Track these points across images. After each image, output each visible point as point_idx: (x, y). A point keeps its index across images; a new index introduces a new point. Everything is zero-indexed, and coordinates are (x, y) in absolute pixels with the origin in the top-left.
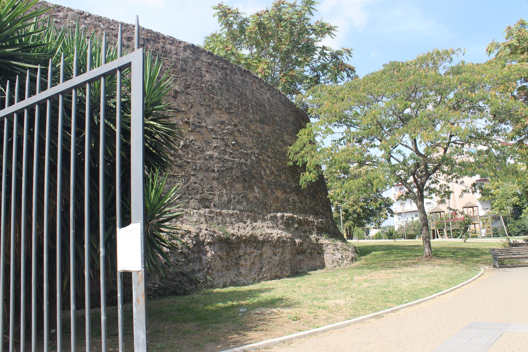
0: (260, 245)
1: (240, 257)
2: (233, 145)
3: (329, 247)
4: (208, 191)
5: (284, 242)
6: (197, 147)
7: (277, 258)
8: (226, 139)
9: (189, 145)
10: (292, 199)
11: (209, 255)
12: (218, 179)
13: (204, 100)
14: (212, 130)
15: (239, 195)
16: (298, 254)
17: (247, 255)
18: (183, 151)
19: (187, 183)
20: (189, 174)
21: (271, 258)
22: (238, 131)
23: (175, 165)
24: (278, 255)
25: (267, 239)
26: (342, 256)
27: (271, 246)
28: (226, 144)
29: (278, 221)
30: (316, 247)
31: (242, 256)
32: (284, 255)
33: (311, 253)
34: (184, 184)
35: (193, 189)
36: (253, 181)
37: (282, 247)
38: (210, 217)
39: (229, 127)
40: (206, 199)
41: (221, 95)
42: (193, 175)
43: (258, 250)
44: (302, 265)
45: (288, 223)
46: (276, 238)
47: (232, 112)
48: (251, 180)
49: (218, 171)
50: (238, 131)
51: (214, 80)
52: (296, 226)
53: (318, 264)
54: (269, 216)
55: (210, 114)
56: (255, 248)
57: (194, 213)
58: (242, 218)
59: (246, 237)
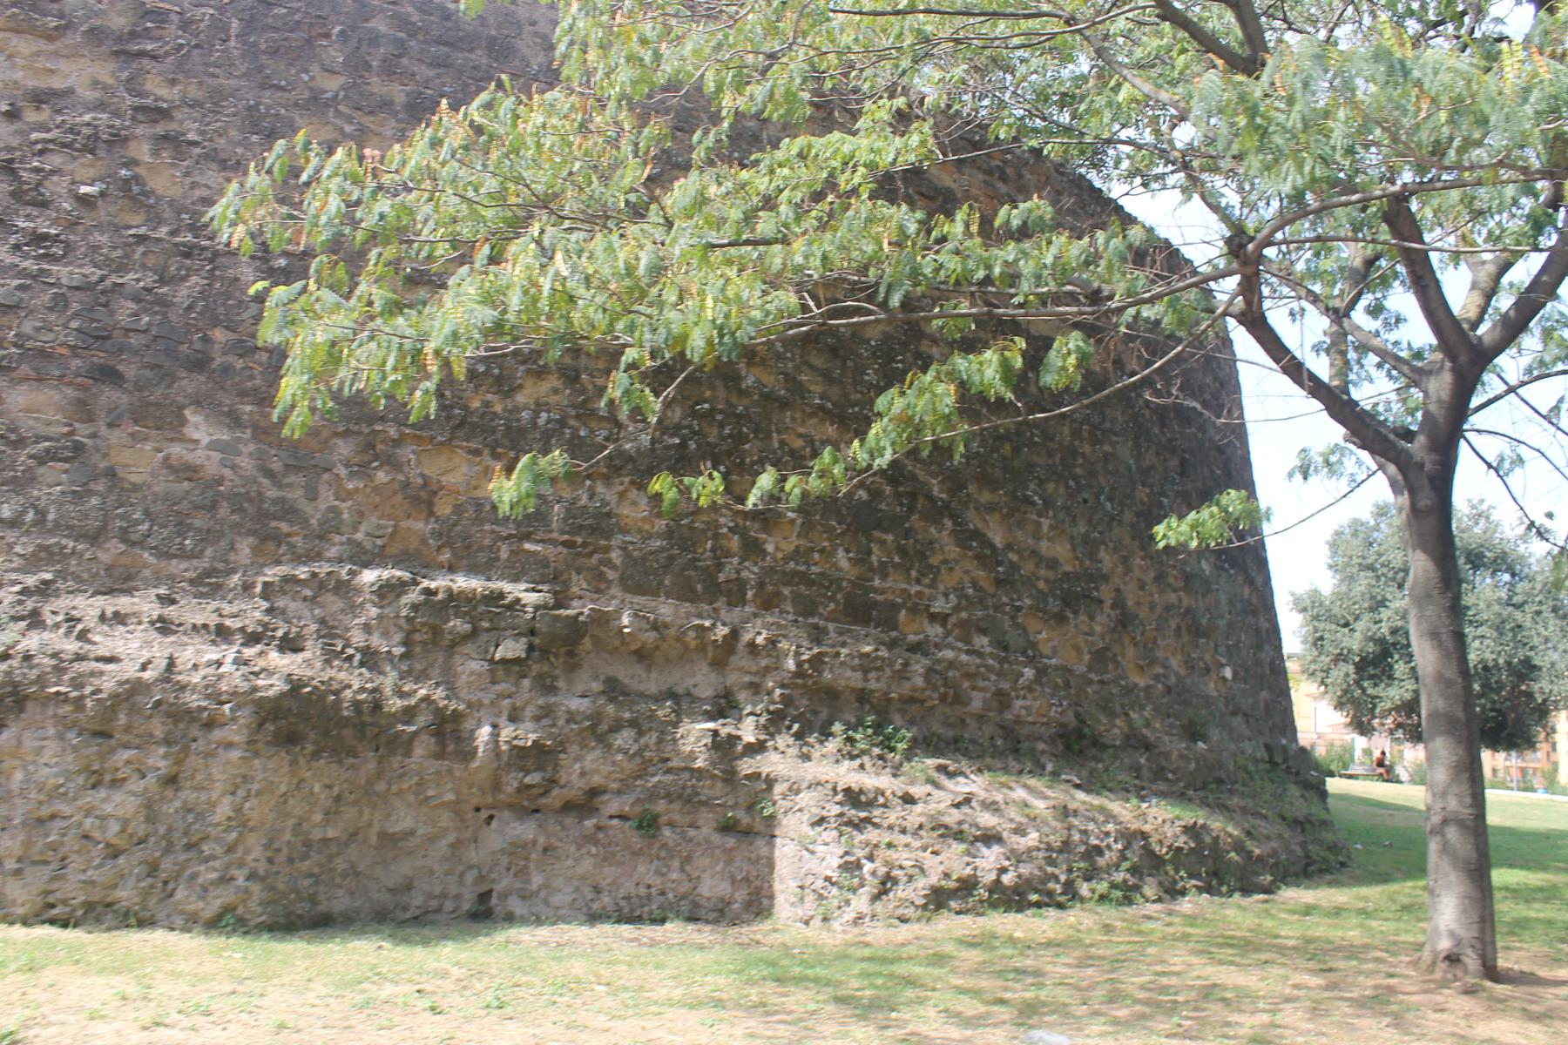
2: (85, 201)
3: (805, 798)
5: (179, 715)
7: (121, 804)
8: (37, 170)
10: (572, 511)
15: (20, 443)
16: (528, 806)
21: (54, 793)
22: (173, 143)
24: (136, 785)
25: (41, 681)
26: (852, 867)
27: (64, 724)
28: (16, 195)
29: (353, 609)
30: (713, 790)
32: (188, 795)
33: (648, 824)
36: (190, 383)
37: (167, 742)
44: (537, 880)
45: (436, 631)
46: (108, 685)
47: (142, 54)
48: (169, 377)
50: (173, 143)
52: (511, 648)
53: (712, 887)
54: (272, 574)
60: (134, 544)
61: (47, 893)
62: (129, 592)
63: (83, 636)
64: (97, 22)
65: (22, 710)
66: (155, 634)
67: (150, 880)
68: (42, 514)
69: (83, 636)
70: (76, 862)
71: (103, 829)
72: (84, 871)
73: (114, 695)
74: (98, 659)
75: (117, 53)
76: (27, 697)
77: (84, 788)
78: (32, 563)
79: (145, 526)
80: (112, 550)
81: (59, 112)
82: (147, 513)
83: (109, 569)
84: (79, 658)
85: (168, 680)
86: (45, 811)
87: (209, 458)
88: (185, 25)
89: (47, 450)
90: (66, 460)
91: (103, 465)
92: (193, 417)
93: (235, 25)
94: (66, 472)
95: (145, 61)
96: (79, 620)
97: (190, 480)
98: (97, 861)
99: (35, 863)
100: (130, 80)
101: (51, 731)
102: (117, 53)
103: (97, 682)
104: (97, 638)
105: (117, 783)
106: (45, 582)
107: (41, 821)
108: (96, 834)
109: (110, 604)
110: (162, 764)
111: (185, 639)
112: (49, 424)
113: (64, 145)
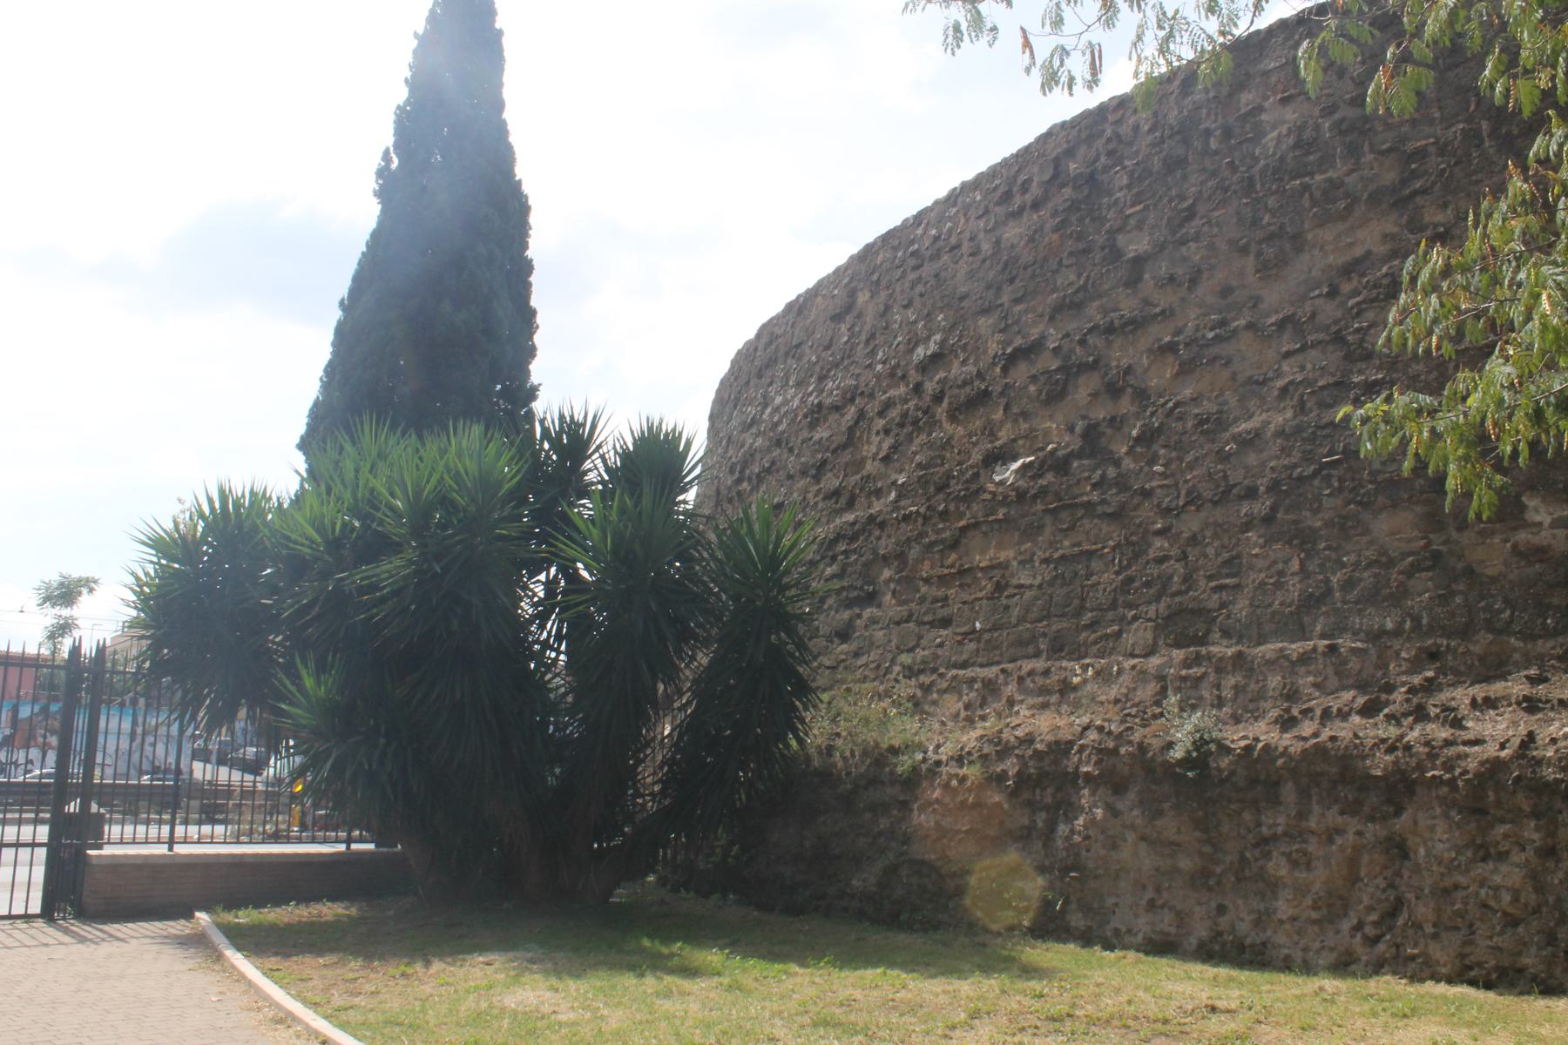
0: (1373, 799)
1: (1264, 841)
4: (1210, 578)
5: (1541, 789)
6: (1190, 424)
7: (1509, 875)
8: (1358, 330)
9: (1160, 430)
11: (1081, 821)
12: (1269, 519)
13: (1255, 222)
14: (1281, 325)
15: (1391, 563)
17: (1313, 840)
18: (1136, 459)
19: (1129, 566)
20: (1146, 531)
23: (1099, 517)
24: (1518, 857)
25: (1420, 767)
28: (1348, 357)
31: (1275, 838)
34: (1117, 573)
35: (1148, 584)
37: (1536, 814)
38: (1184, 679)
39: (1384, 270)
40: (1193, 612)
41: (1353, 151)
42: (1159, 533)
43: (1372, 819)
46: (1472, 765)
47: (1415, 193)
49: (1274, 487)
51: (1317, 112)
55: (1282, 261)
56: (1352, 809)
57: (1120, 672)
58: (1386, 666)
59: (1290, 757)
60: (1500, 632)
61: (1463, 956)
62: (1503, 677)
63: (1457, 723)
64: (1372, 187)
65: (1413, 793)
66: (1522, 714)
67: (1550, 949)
68: (1416, 619)
69: (1457, 723)
70: (1482, 930)
71: (1497, 897)
72: (1491, 938)
73: (1478, 775)
74: (1465, 743)
75: (1395, 205)
76: (1414, 782)
77: (1473, 861)
78: (1415, 666)
79: (1508, 612)
80: (1481, 642)
81: (1363, 275)
82: (1506, 601)
83: (1482, 659)
84: (1448, 743)
85: (1523, 756)
86: (1448, 882)
87: (1554, 536)
88: (1442, 151)
89: (1412, 564)
90: (1428, 569)
91: (1460, 566)
92: (1531, 502)
93: (1485, 125)
94: (1431, 579)
95: (1418, 199)
96: (1454, 709)
97: (1541, 561)
98: (1498, 928)
99: (1448, 929)
100: (1410, 221)
101: (1438, 810)
102: (1395, 205)
103: (1463, 764)
104: (1470, 724)
105: (1502, 856)
106: (1427, 679)
107: (1446, 892)
108: (1492, 903)
109: (1479, 691)
110: (1536, 836)
111: (1552, 714)
112: (1409, 541)
113: (1373, 301)
